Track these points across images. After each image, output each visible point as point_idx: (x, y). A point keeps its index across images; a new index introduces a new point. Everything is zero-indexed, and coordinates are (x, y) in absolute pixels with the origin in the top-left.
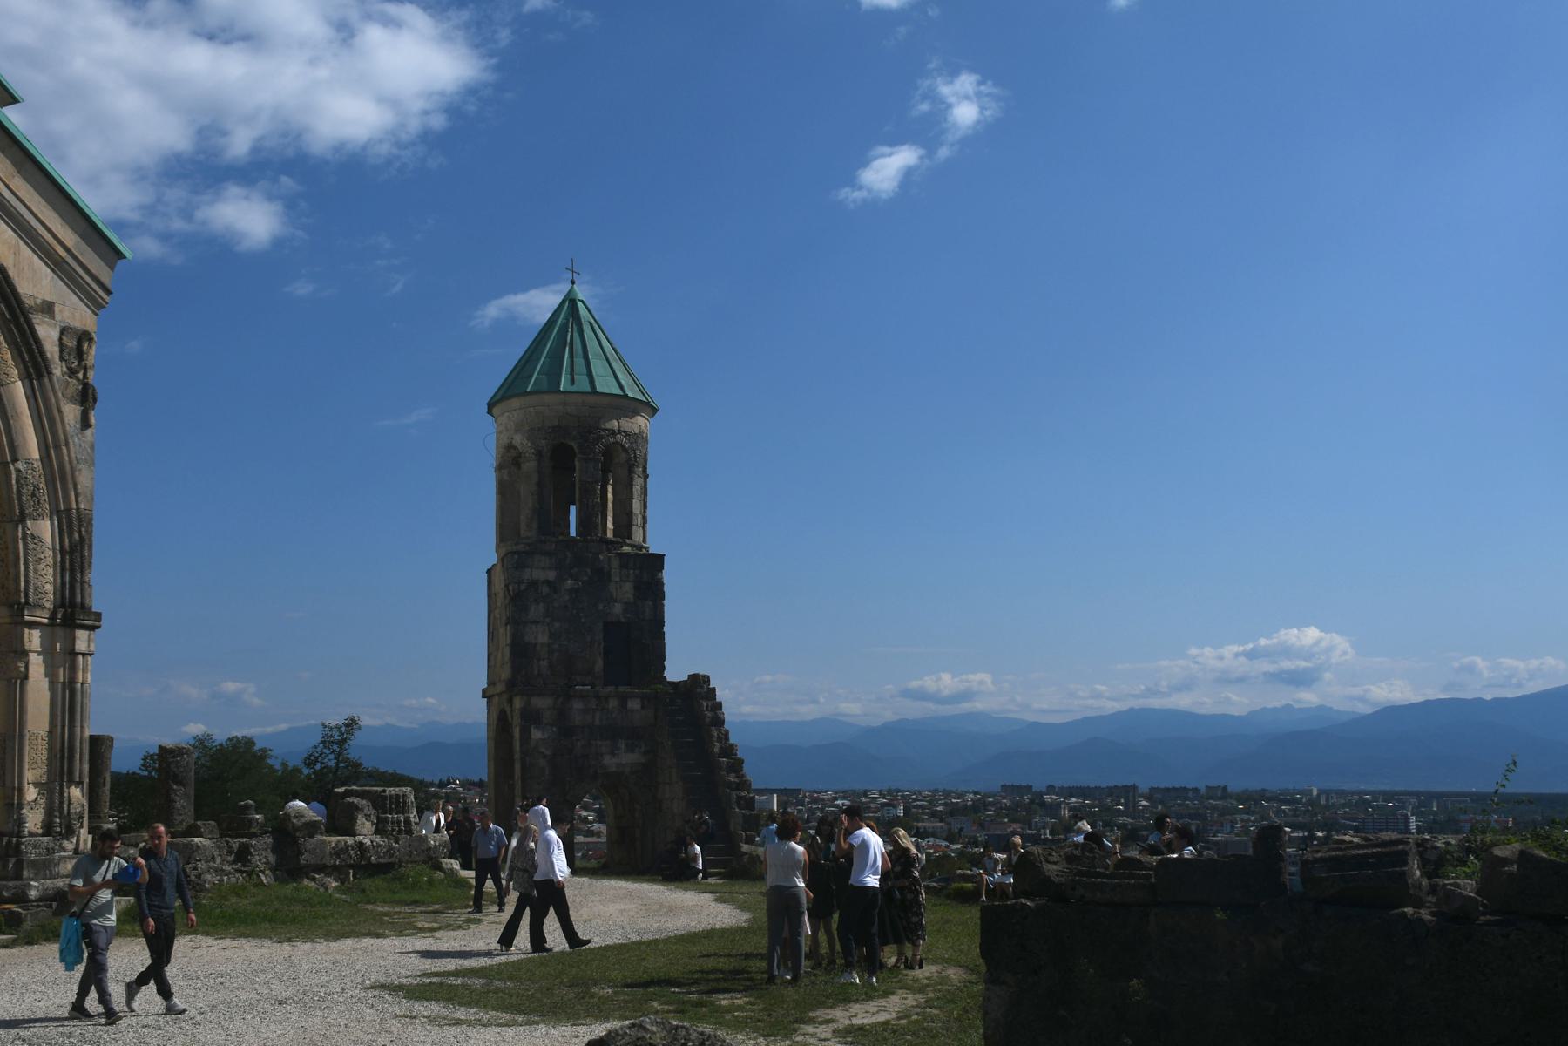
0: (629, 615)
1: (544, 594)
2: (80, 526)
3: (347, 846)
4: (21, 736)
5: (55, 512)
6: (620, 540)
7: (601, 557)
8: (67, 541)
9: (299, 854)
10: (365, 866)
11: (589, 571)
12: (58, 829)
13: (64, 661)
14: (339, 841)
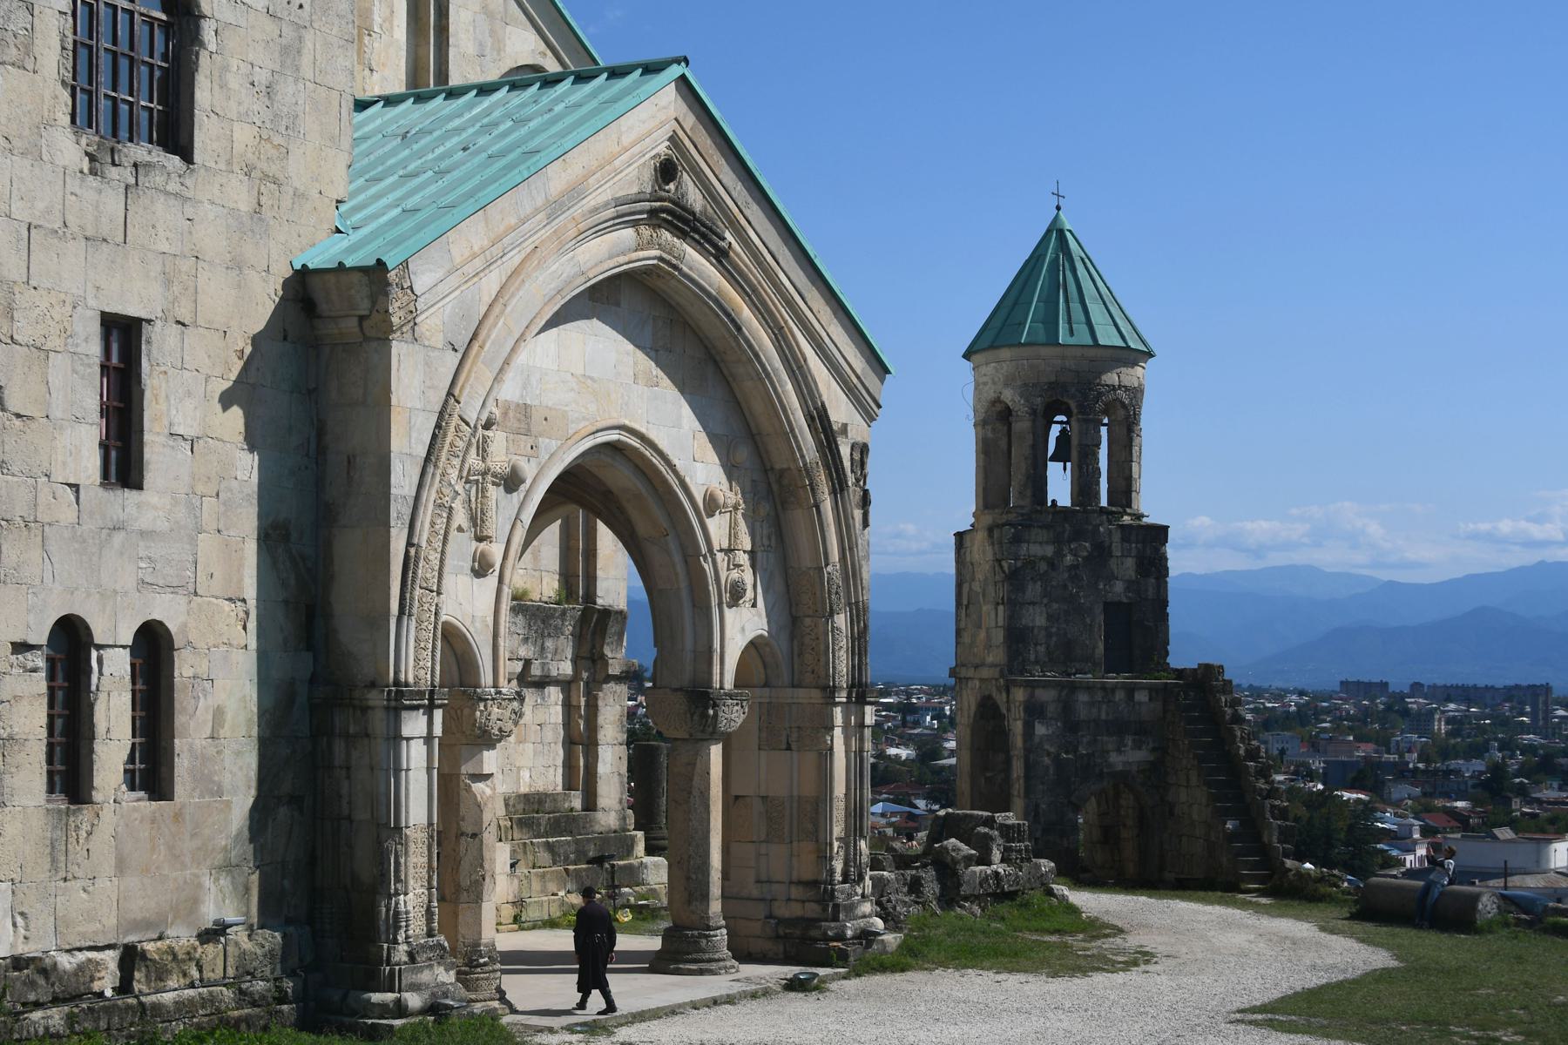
3: (987, 876)
6: (1120, 510)
7: (1101, 529)
10: (999, 894)
14: (981, 872)
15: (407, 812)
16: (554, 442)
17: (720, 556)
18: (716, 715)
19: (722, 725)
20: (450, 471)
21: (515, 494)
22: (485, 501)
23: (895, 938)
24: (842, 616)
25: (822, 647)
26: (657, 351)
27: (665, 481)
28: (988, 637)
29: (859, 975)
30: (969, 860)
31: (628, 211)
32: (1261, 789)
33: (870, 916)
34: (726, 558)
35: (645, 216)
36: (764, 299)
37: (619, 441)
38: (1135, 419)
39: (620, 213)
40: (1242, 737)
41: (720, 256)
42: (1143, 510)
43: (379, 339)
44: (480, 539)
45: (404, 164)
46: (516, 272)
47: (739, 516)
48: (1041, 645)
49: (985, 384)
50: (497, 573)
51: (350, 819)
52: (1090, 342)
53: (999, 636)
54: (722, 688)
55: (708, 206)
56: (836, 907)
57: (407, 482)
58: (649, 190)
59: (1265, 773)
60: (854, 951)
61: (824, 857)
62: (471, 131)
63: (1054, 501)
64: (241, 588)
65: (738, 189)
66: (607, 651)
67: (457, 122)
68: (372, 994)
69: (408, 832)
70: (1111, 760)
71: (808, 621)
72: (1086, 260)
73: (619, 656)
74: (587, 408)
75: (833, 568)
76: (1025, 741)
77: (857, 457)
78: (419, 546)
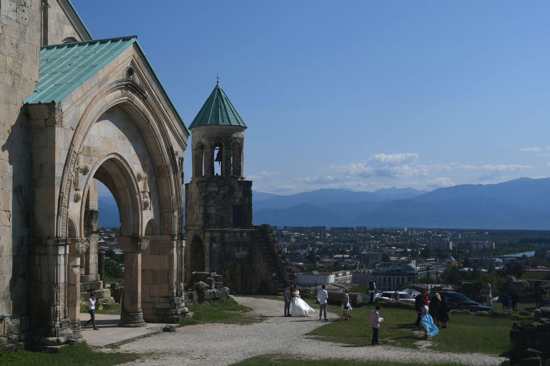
0: (241, 203)
1: (214, 196)
3: (211, 293)
4: (173, 270)
6: (238, 176)
7: (232, 182)
9: (204, 296)
10: (215, 298)
11: (228, 187)
12: (179, 295)
15: (60, 279)
16: (96, 159)
17: (141, 194)
18: (140, 244)
19: (142, 248)
20: (71, 168)
21: (86, 175)
22: (78, 178)
23: (192, 314)
24: (176, 212)
25: (170, 222)
26: (124, 129)
27: (126, 170)
28: (197, 216)
29: (183, 326)
30: (207, 288)
31: (120, 85)
32: (283, 263)
33: (184, 307)
34: (143, 195)
35: (124, 86)
36: (156, 112)
37: (114, 158)
38: (242, 148)
39: (118, 85)
40: (276, 247)
41: (144, 99)
42: (244, 176)
43: (51, 126)
44: (76, 190)
45: (50, 69)
46: (89, 105)
48: (214, 219)
49: (196, 137)
50: (81, 201)
51: (41, 281)
52: (229, 124)
53: (201, 216)
54: (142, 236)
55: (141, 83)
56: (175, 304)
57: (60, 173)
58: (125, 78)
59: (283, 258)
60: (181, 318)
61: (171, 289)
62: (69, 59)
63: (217, 174)
65: (149, 77)
66: (93, 224)
67: (63, 56)
68: (49, 338)
69: (60, 285)
70: (236, 254)
71: (166, 214)
72: (227, 98)
73: (96, 225)
74: (105, 148)
75: (174, 197)
76: (210, 249)
77: (180, 162)
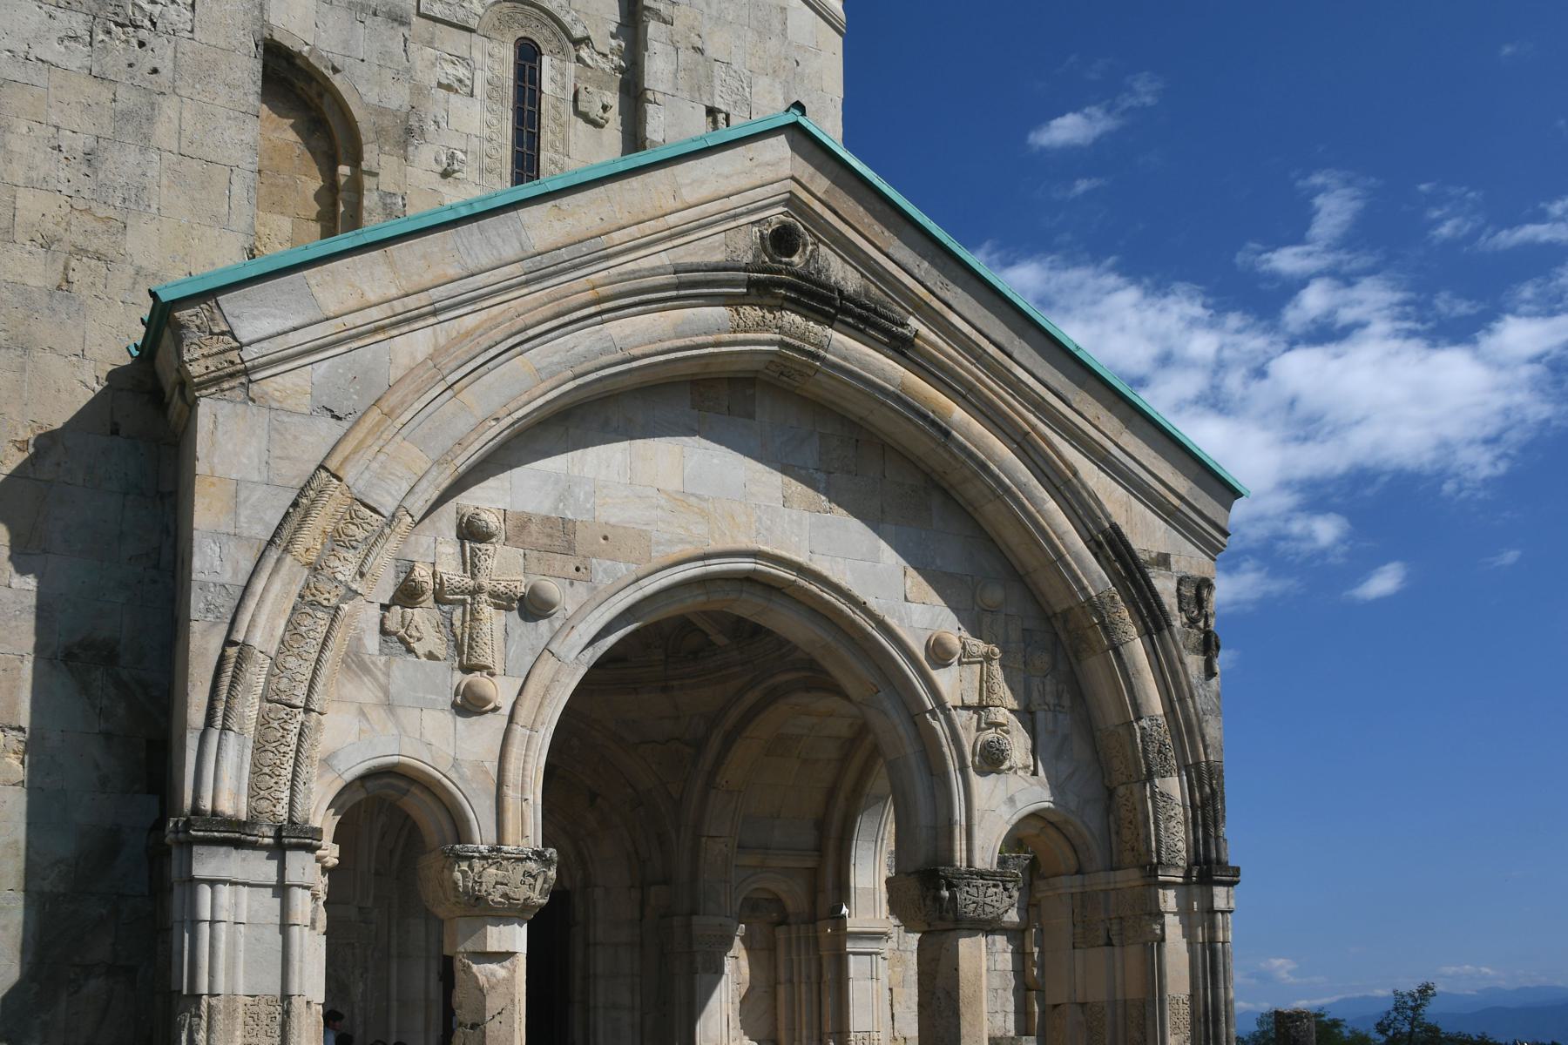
2: (1211, 779)
5: (1182, 766)
8: (1197, 795)
13: (1202, 920)
18: (953, 898)
25: (1140, 817)
34: (976, 716)
47: (996, 666)
64: (13, 707)
71: (1122, 790)
78: (244, 647)
